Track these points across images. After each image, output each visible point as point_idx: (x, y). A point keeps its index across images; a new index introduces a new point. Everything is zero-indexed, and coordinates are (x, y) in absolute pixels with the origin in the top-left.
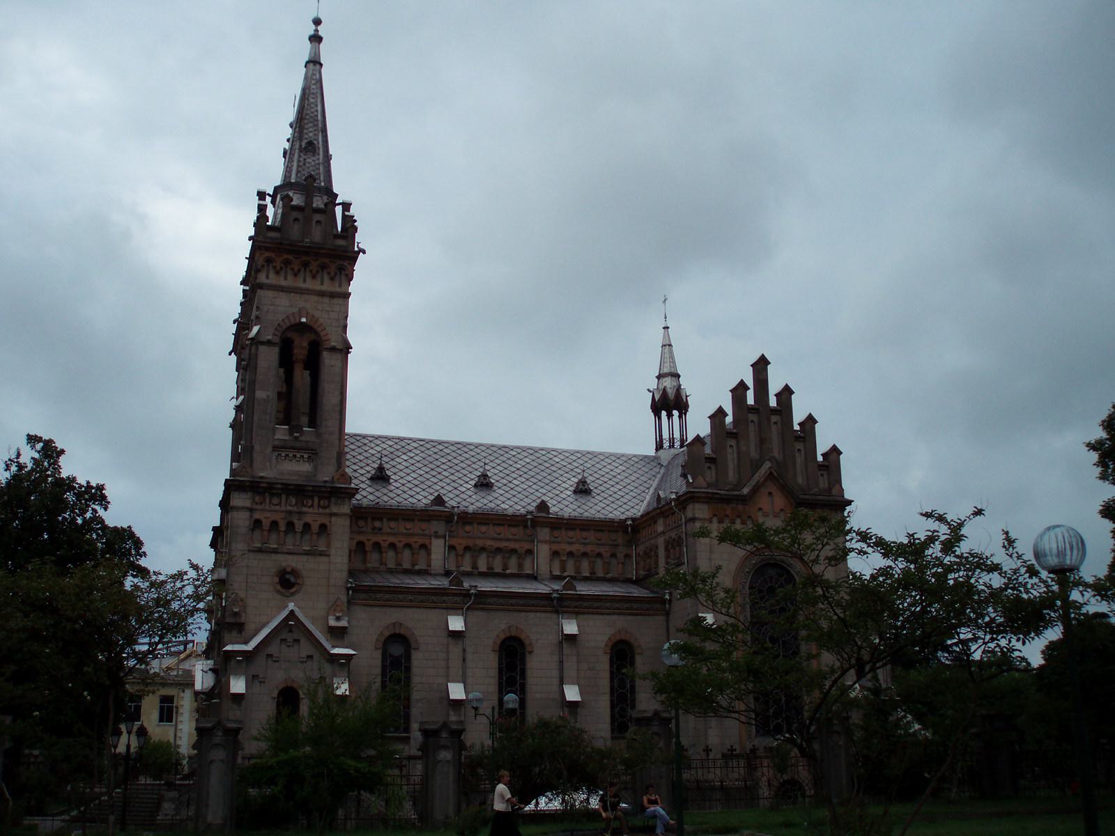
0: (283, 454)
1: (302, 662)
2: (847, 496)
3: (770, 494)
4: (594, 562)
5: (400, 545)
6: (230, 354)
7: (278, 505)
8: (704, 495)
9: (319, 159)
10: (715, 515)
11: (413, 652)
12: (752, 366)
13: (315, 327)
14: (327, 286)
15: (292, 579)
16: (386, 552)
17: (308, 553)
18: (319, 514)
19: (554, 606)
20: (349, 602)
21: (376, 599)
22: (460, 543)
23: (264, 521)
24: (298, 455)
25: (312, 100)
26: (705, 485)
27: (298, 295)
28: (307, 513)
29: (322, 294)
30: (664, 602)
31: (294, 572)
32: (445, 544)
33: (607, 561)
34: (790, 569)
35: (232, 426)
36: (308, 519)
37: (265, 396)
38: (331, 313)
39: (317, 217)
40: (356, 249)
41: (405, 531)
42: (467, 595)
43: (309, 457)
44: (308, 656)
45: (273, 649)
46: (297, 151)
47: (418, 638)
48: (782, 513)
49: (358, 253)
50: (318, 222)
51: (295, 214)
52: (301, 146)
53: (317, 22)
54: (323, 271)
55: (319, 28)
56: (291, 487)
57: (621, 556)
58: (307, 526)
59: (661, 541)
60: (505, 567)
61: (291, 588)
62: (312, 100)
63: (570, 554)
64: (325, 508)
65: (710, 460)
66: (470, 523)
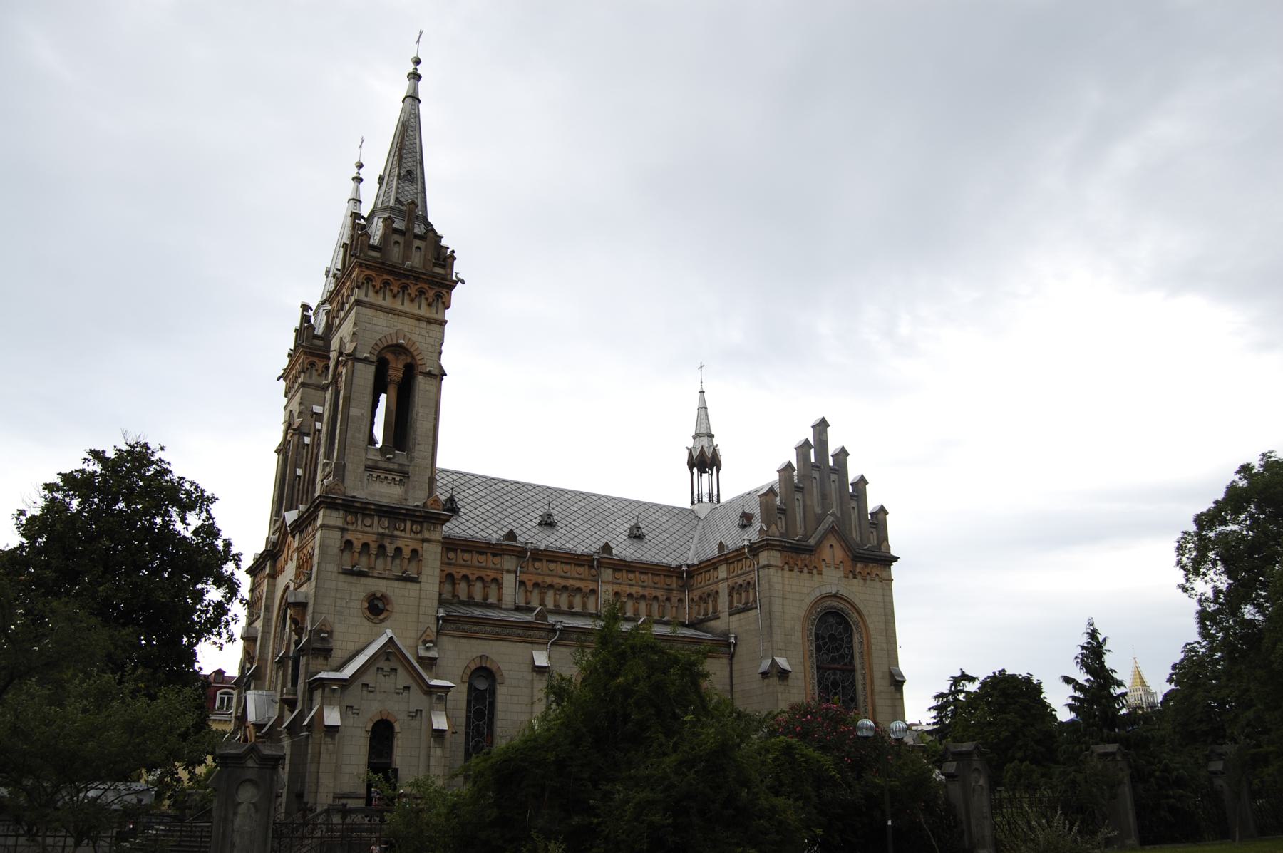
0: (375, 475)
1: (398, 693)
2: (893, 552)
3: (831, 546)
4: (651, 605)
5: (472, 578)
6: (278, 379)
7: (369, 526)
8: (778, 543)
9: (417, 189)
10: (786, 563)
11: (498, 686)
12: (813, 427)
13: (412, 350)
14: (424, 311)
15: (381, 605)
16: (459, 584)
17: (399, 579)
18: (411, 539)
20: (438, 632)
21: (464, 631)
22: (530, 579)
23: (355, 542)
24: (390, 477)
25: (411, 133)
26: (777, 534)
27: (396, 317)
28: (400, 537)
29: (419, 318)
30: (729, 645)
31: (384, 598)
32: (516, 579)
33: (662, 604)
34: (848, 618)
35: (278, 451)
36: (400, 543)
37: (359, 415)
38: (427, 338)
39: (417, 243)
40: (454, 278)
41: (477, 564)
42: (552, 630)
43: (401, 480)
44: (405, 687)
45: (367, 679)
46: (396, 178)
47: (504, 672)
48: (841, 564)
49: (457, 282)
50: (418, 248)
51: (396, 237)
52: (399, 174)
53: (417, 62)
54: (421, 295)
55: (418, 67)
56: (385, 509)
57: (674, 600)
58: (398, 550)
59: (723, 588)
60: (571, 606)
61: (379, 615)
62: (411, 133)
63: (630, 596)
64: (417, 533)
65: (782, 511)
66: (540, 560)
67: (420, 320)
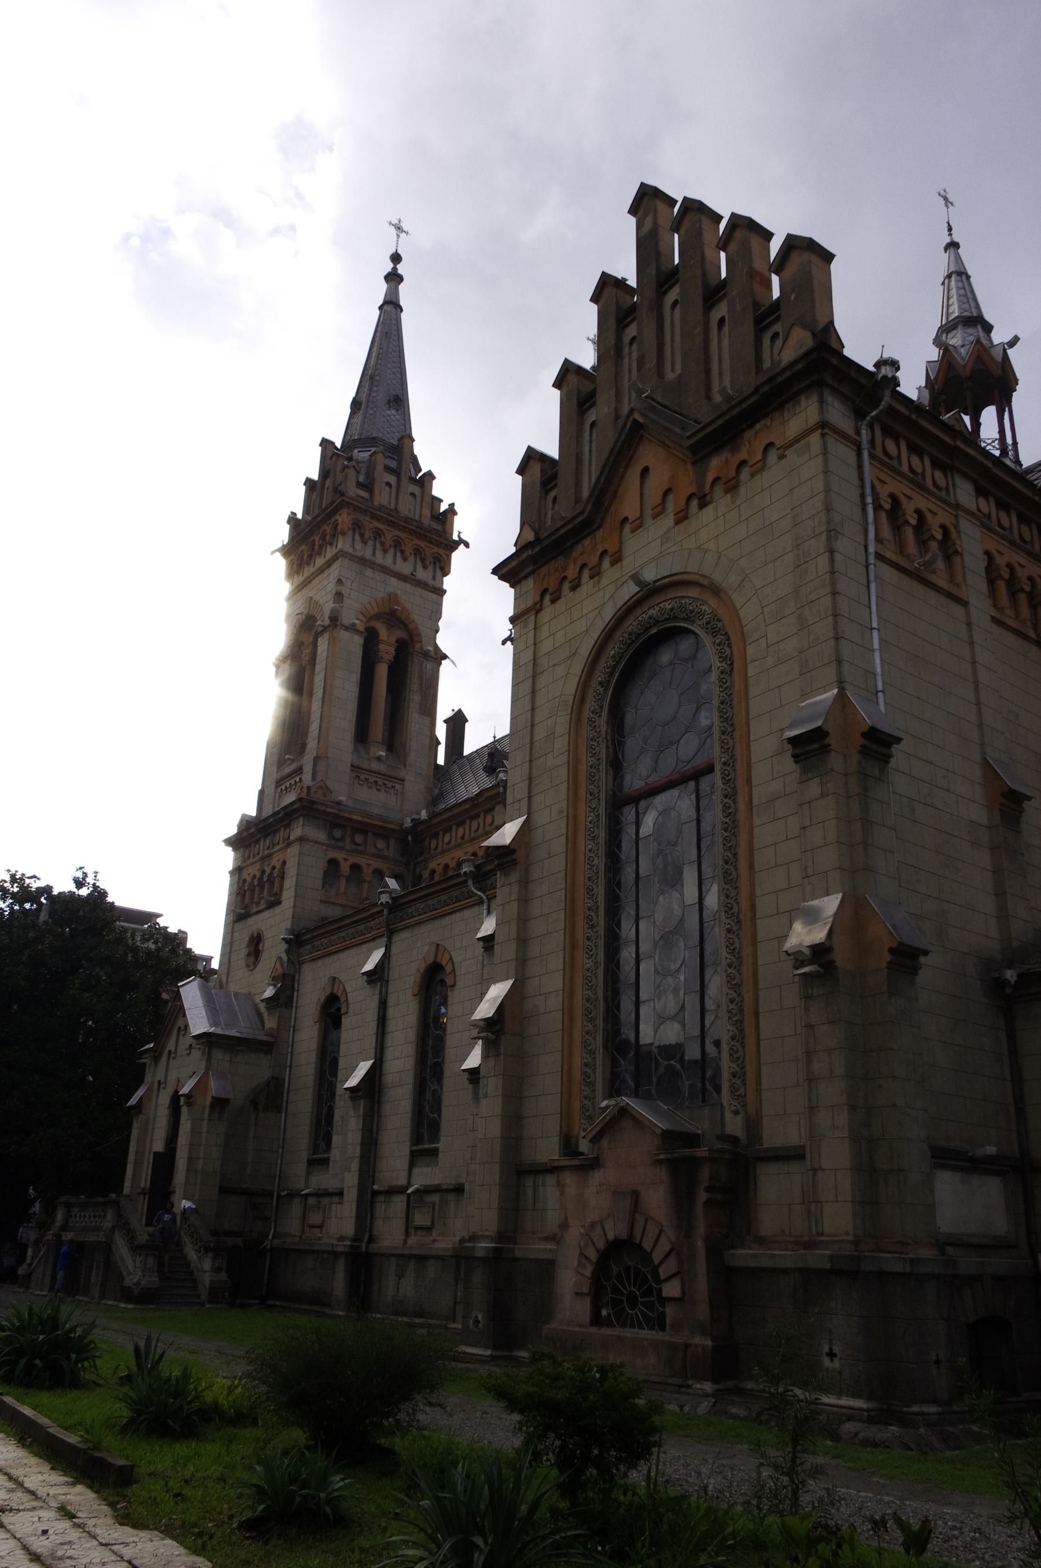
40: (455, 537)
55: (398, 266)
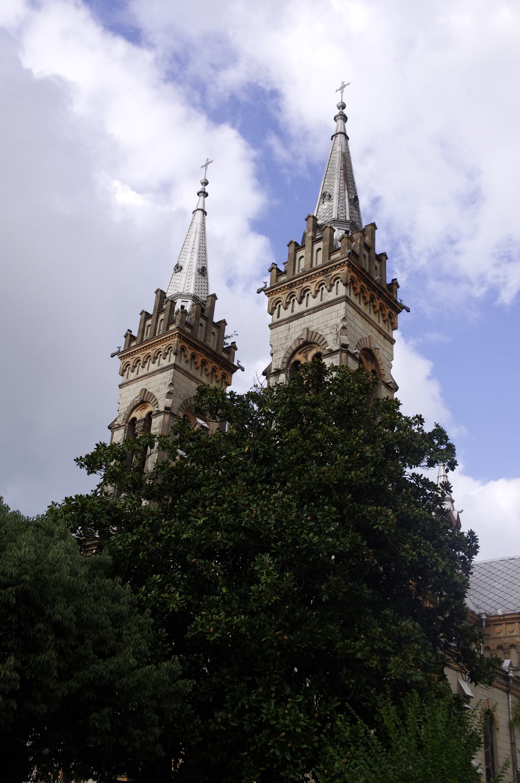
19: (507, 686)
27: (367, 323)
53: (343, 106)
67: (380, 333)
